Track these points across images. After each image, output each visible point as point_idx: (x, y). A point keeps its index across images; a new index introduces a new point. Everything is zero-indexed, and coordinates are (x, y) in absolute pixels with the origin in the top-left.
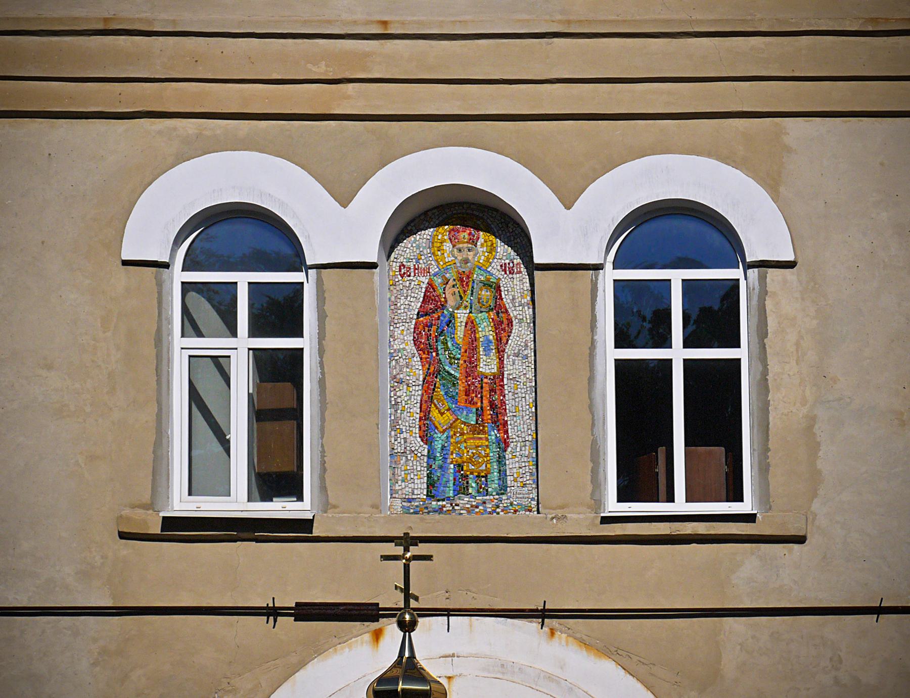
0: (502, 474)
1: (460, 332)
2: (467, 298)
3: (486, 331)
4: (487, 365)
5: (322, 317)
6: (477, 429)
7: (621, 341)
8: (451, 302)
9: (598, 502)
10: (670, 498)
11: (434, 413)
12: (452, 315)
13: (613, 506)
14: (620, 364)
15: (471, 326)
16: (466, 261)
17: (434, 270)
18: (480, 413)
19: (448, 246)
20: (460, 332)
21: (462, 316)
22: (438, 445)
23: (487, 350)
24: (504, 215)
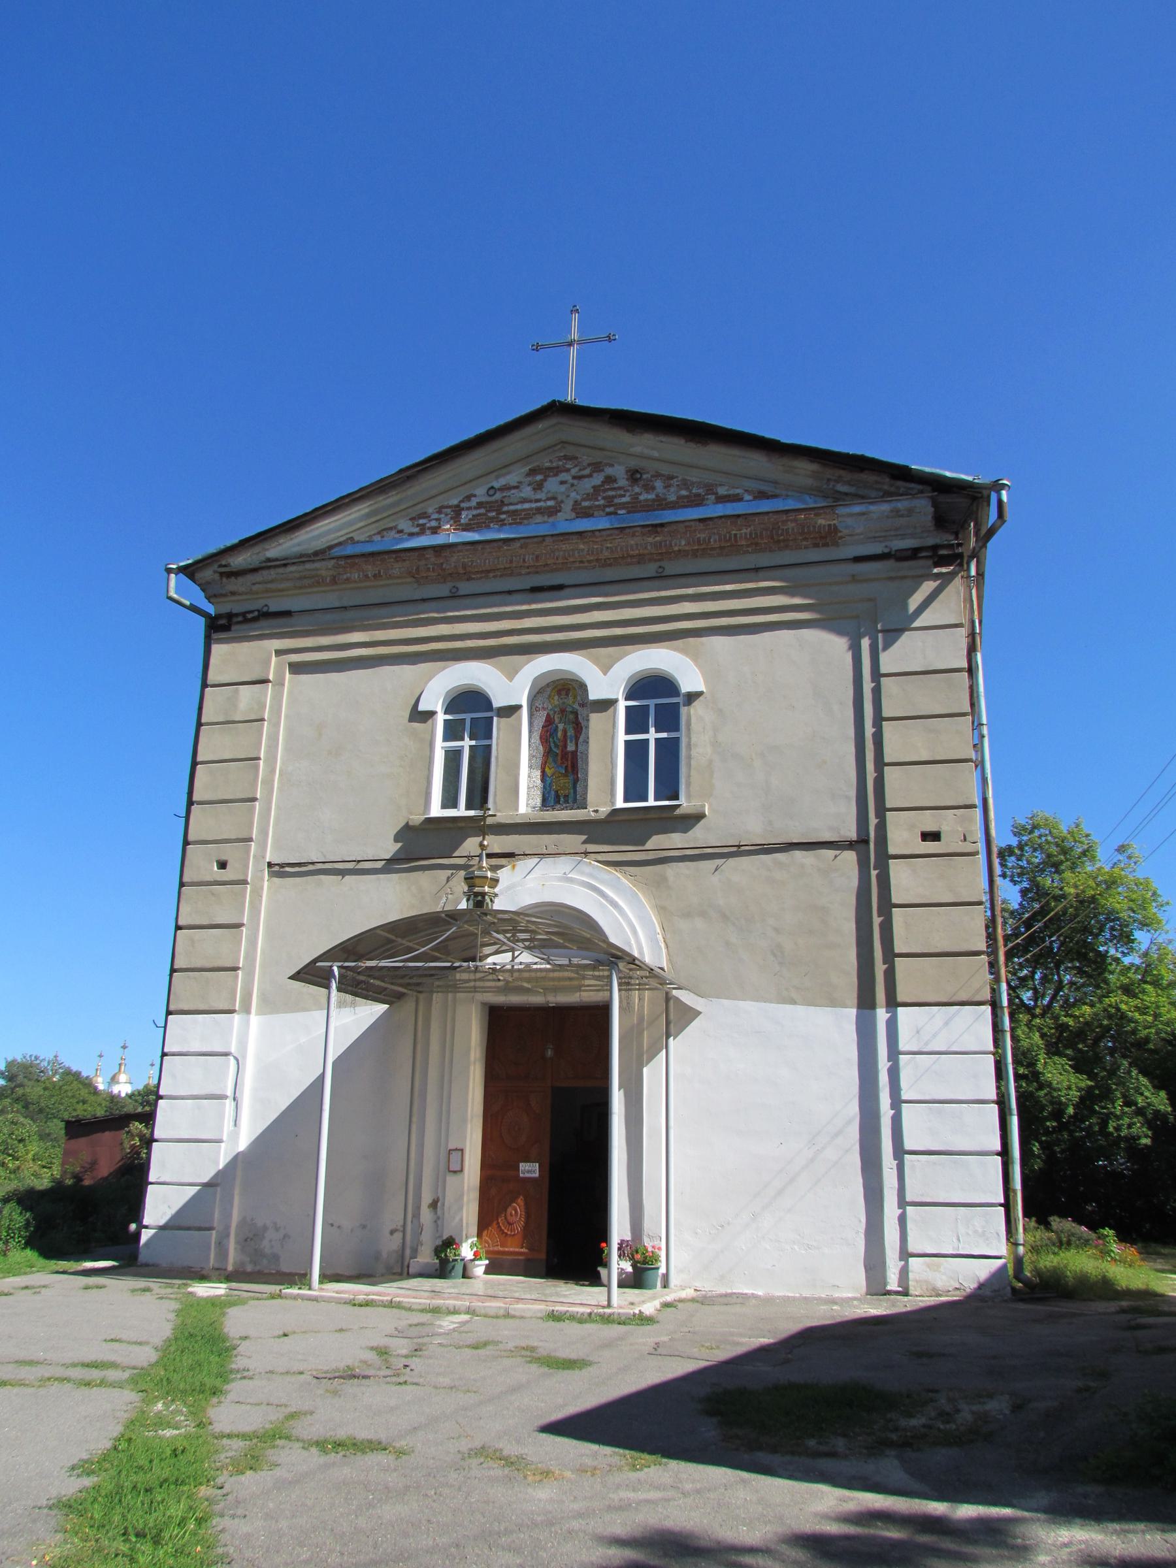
0: (575, 792)
1: (560, 734)
2: (563, 719)
3: (571, 732)
4: (571, 747)
5: (498, 729)
6: (566, 775)
7: (628, 732)
8: (557, 720)
9: (613, 803)
10: (646, 800)
11: (547, 769)
12: (557, 727)
13: (620, 803)
14: (627, 743)
15: (565, 731)
16: (564, 703)
17: (550, 707)
18: (566, 767)
19: (556, 697)
20: (560, 734)
21: (561, 726)
22: (548, 782)
23: (571, 742)
24: (580, 682)
